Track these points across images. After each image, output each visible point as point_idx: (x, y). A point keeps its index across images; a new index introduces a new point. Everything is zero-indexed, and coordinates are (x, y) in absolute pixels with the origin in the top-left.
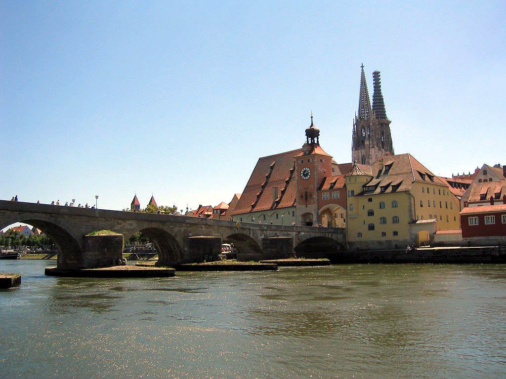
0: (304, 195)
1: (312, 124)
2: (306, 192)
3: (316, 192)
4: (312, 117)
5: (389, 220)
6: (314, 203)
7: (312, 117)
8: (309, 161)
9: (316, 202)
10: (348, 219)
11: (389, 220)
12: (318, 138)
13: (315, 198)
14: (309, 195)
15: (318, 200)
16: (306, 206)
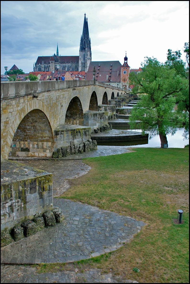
8: (126, 69)
12: (127, 61)
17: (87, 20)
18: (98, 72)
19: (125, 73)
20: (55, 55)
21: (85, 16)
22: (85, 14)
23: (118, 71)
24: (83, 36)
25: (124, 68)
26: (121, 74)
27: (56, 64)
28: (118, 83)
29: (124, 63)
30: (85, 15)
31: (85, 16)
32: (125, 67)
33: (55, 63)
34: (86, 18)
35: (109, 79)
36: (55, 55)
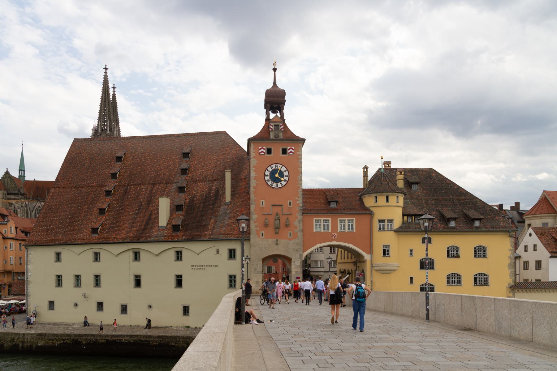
0: (271, 219)
1: (275, 83)
2: (277, 214)
3: (300, 217)
4: (275, 70)
5: (467, 280)
6: (295, 236)
7: (275, 70)
8: (284, 151)
9: (300, 235)
10: (375, 273)
11: (467, 280)
13: (296, 227)
14: (283, 219)
15: (303, 231)
16: (277, 241)
17: (114, 91)
18: (107, 189)
19: (277, 180)
20: (7, 173)
21: (106, 73)
22: (105, 67)
23: (228, 175)
24: (98, 124)
25: (269, 151)
26: (253, 183)
27: (10, 201)
28: (236, 246)
29: (268, 120)
30: (106, 69)
31: (106, 73)
32: (277, 139)
33: (8, 199)
34: (111, 85)
35: (174, 223)
36: (7, 173)
